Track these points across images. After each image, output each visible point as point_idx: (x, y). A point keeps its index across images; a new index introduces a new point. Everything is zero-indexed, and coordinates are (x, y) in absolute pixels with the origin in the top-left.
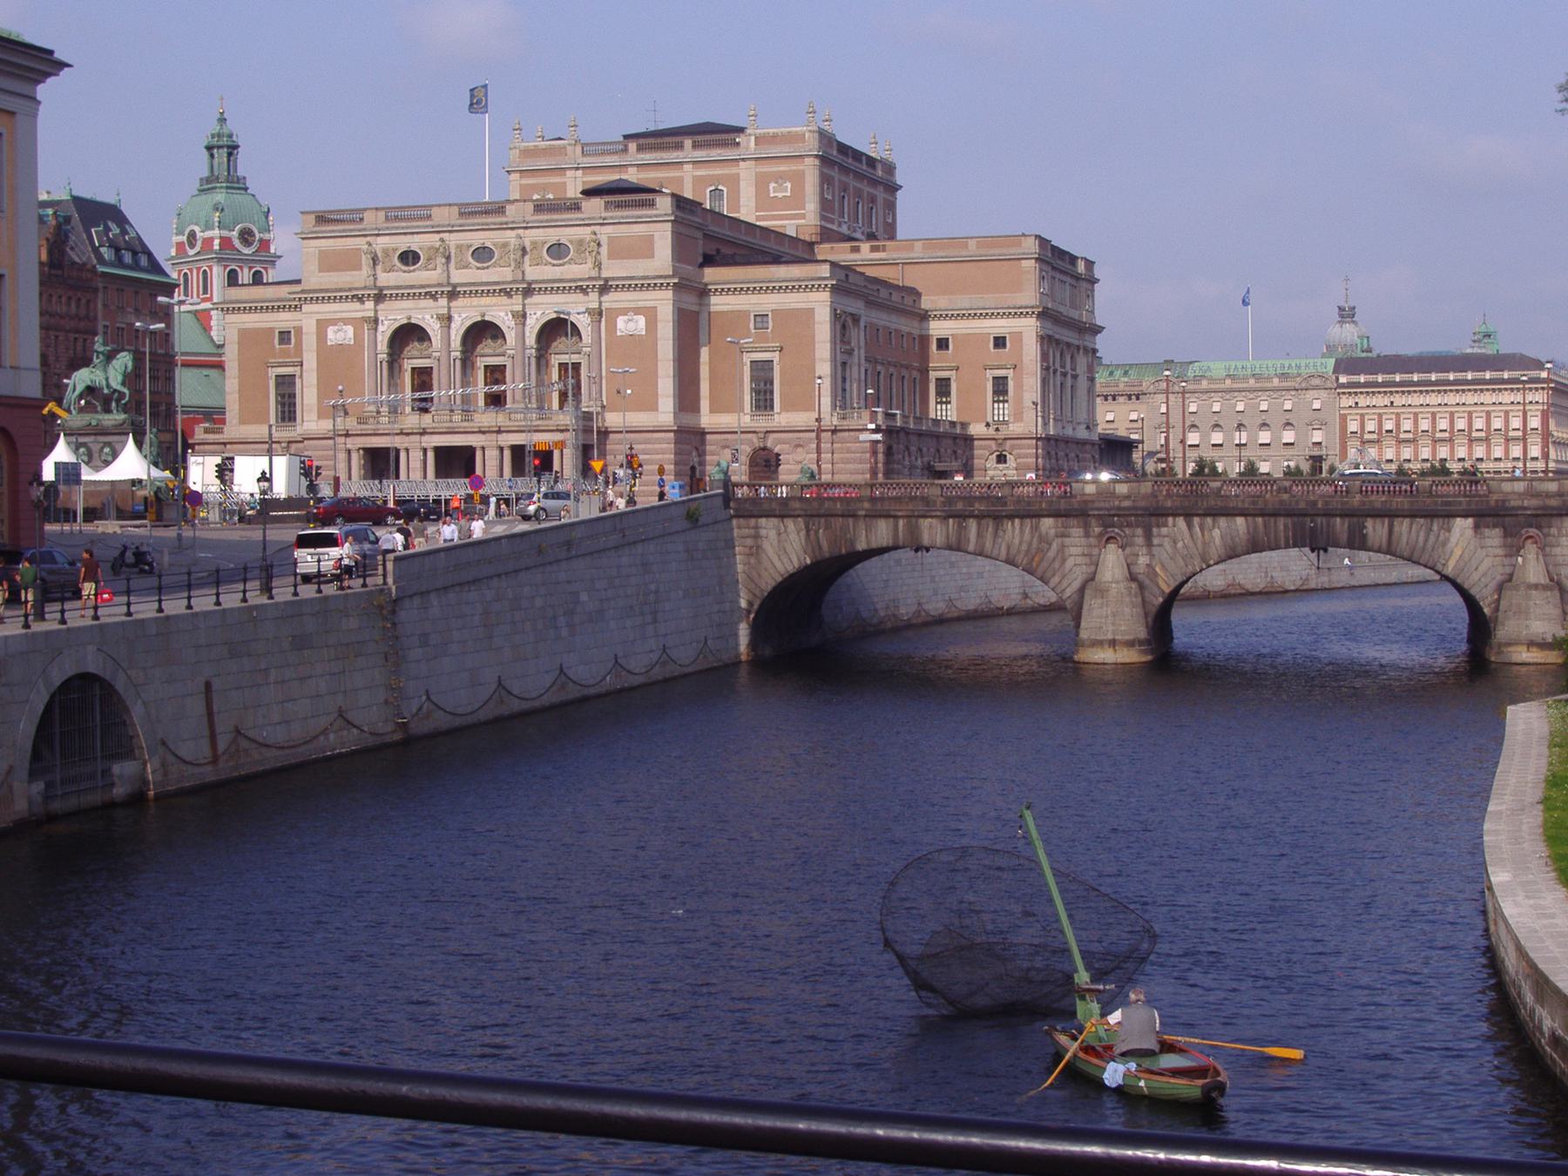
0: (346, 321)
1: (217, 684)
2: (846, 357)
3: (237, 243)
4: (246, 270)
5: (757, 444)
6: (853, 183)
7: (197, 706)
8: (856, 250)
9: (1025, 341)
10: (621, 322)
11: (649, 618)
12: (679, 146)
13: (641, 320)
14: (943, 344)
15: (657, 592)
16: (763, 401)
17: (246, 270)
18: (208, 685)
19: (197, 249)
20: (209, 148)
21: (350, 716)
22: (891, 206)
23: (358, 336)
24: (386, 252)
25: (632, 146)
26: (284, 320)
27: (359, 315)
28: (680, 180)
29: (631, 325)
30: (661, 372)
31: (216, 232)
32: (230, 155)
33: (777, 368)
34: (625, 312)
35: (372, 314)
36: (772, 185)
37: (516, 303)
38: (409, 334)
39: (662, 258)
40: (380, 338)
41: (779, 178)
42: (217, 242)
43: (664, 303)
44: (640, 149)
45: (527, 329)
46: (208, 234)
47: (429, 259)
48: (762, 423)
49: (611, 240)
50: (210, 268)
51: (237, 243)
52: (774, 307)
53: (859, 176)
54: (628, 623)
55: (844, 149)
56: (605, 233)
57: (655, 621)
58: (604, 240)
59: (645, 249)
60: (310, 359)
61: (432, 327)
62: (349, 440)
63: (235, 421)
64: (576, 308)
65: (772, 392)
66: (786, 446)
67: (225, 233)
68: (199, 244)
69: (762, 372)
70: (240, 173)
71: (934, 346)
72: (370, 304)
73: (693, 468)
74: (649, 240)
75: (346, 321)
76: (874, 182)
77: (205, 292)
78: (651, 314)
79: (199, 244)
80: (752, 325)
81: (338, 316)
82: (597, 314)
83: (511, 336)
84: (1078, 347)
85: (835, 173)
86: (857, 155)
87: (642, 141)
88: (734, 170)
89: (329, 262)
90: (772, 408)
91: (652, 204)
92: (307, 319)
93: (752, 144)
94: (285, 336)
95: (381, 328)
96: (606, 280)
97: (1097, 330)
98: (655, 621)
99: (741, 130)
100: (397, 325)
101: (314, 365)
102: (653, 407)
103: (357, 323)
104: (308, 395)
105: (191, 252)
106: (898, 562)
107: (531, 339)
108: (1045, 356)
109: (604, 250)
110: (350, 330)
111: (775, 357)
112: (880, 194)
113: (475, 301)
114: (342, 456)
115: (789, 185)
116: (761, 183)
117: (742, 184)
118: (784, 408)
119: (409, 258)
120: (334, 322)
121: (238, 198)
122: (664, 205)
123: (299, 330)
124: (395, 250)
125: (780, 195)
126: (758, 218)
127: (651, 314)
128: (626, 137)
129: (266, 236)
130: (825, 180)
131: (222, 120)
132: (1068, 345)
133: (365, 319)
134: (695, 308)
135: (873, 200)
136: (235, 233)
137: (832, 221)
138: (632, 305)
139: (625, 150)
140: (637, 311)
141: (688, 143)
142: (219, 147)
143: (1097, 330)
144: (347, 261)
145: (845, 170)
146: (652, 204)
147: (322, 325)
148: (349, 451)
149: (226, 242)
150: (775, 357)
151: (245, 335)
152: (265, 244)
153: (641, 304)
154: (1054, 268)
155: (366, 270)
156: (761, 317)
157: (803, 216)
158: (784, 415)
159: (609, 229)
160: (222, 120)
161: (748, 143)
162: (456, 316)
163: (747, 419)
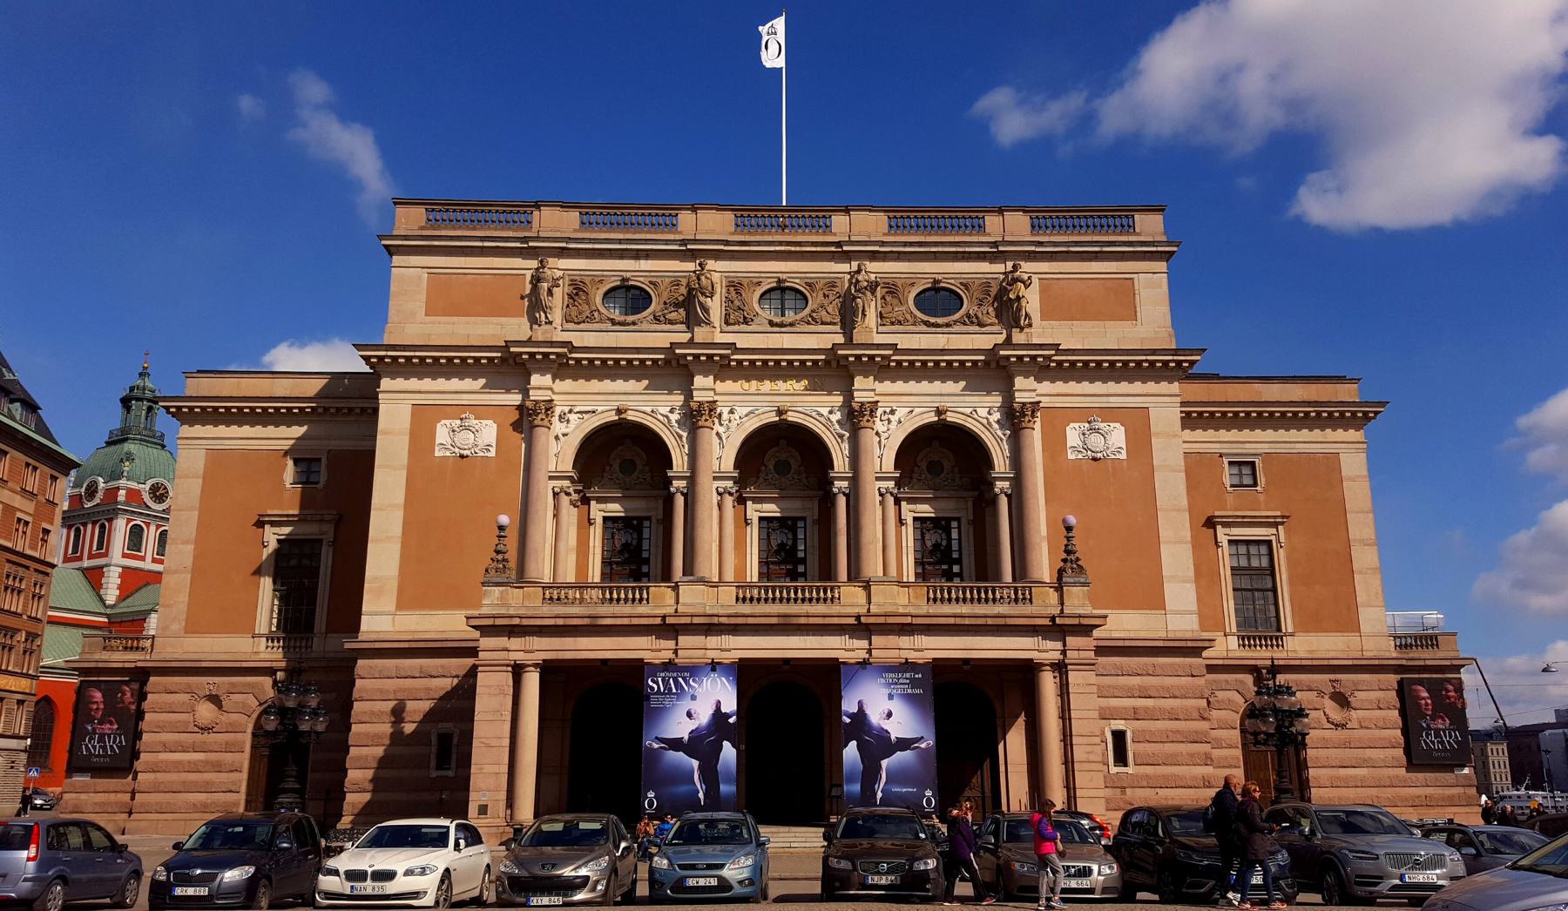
3: (146, 498)
4: (153, 528)
17: (153, 528)
20: (126, 402)
24: (578, 290)
29: (1096, 441)
32: (150, 409)
33: (1281, 556)
48: (1261, 655)
51: (146, 498)
52: (1265, 448)
62: (515, 643)
67: (133, 485)
68: (100, 495)
75: (481, 411)
77: (100, 546)
78: (1138, 424)
79: (100, 495)
80: (1227, 481)
89: (442, 301)
95: (558, 427)
101: (400, 496)
102: (1154, 599)
119: (633, 298)
121: (155, 452)
136: (147, 487)
140: (1110, 414)
142: (138, 399)
147: (424, 418)
148: (518, 671)
150: (1279, 536)
156: (1245, 466)
159: (1044, 266)
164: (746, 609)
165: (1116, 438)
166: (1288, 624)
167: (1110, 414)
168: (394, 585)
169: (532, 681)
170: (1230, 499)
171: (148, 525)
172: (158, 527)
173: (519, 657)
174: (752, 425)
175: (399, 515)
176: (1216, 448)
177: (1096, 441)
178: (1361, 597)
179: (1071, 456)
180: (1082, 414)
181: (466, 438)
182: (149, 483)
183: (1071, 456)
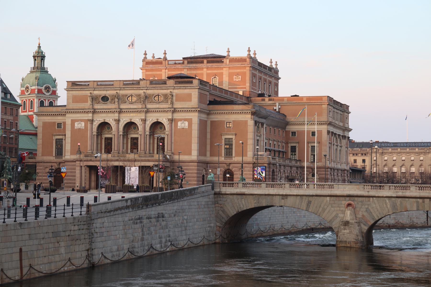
0: (82, 120)
1: (24, 249)
2: (258, 138)
4: (47, 101)
5: (226, 167)
6: (263, 76)
7: (16, 257)
8: (264, 100)
9: (323, 134)
10: (179, 124)
11: (183, 228)
12: (202, 62)
13: (187, 123)
14: (294, 133)
15: (187, 219)
16: (229, 153)
17: (47, 101)
18: (21, 250)
19: (29, 93)
20: (34, 57)
21: (72, 261)
22: (277, 85)
23: (86, 126)
25: (186, 62)
26: (59, 119)
27: (87, 118)
28: (202, 74)
29: (183, 125)
30: (193, 141)
31: (36, 87)
32: (42, 59)
34: (180, 120)
35: (91, 118)
36: (235, 77)
37: (143, 116)
38: (104, 126)
39: (194, 101)
40: (94, 127)
41: (238, 74)
42: (36, 90)
43: (195, 117)
44: (188, 63)
45: (146, 125)
46: (33, 88)
47: (112, 99)
48: (228, 161)
49: (177, 95)
50: (34, 99)
51: (44, 91)
52: (234, 119)
53: (266, 74)
54: (176, 230)
55: (260, 64)
56: (175, 92)
57: (186, 229)
58: (174, 94)
59: (188, 98)
60: (68, 134)
61: (113, 124)
62: (81, 163)
63: (40, 155)
64: (164, 119)
65: (232, 149)
66: (236, 169)
67: (40, 88)
69: (229, 143)
70: (45, 66)
71: (291, 135)
72: (90, 115)
73: (203, 176)
74: (190, 95)
75: (82, 120)
76: (271, 76)
78: (190, 121)
81: (79, 118)
82: (171, 121)
83: (140, 128)
84: (343, 136)
85: (257, 73)
86: (265, 67)
87: (189, 60)
88: (221, 71)
90: (232, 154)
91: (191, 82)
92: (68, 119)
93: (228, 62)
94: (59, 125)
95: (94, 123)
96: (175, 109)
97: (350, 130)
98: (186, 229)
99: (224, 57)
100: (100, 122)
102: (190, 154)
103: (86, 121)
104: (67, 146)
105: (26, 94)
106: (274, 211)
107: (148, 129)
108: (330, 139)
109: (174, 98)
110: (83, 124)
111: (233, 137)
112: (273, 80)
113: (128, 115)
114: (78, 169)
115: (240, 77)
116: (231, 76)
117: (224, 76)
118: (237, 155)
120: (77, 121)
121: (45, 75)
122: (196, 82)
123: (65, 123)
124: (100, 96)
125: (237, 80)
126: (229, 88)
127: (190, 121)
128: (184, 58)
129: (54, 89)
130: (253, 76)
131: (39, 47)
132: (339, 135)
133: (89, 120)
134: (206, 119)
135: (270, 83)
136: (43, 88)
137: (256, 90)
138: (183, 118)
139: (183, 63)
140: (185, 120)
141: (205, 61)
142: (38, 57)
143: (350, 130)
144: (83, 99)
145: (260, 72)
146: (191, 82)
147: (73, 122)
149: (40, 91)
151: (45, 125)
152: (54, 93)
153: (187, 117)
154: (334, 108)
155: (89, 102)
157: (245, 88)
158: (236, 158)
160: (39, 47)
161: (227, 61)
162: (121, 120)
163: (223, 159)
164: (113, 158)
165: (186, 125)
166: (234, 155)
167: (185, 120)
168: (70, 151)
169: (83, 169)
170: (226, 130)
171: (45, 100)
172: (48, 100)
173: (81, 165)
174: (125, 122)
175: (70, 139)
176: (224, 119)
177: (183, 125)
178: (248, 150)
179: (179, 128)
180: (180, 120)
181: (79, 126)
182: (44, 86)
183: (179, 128)
